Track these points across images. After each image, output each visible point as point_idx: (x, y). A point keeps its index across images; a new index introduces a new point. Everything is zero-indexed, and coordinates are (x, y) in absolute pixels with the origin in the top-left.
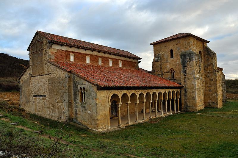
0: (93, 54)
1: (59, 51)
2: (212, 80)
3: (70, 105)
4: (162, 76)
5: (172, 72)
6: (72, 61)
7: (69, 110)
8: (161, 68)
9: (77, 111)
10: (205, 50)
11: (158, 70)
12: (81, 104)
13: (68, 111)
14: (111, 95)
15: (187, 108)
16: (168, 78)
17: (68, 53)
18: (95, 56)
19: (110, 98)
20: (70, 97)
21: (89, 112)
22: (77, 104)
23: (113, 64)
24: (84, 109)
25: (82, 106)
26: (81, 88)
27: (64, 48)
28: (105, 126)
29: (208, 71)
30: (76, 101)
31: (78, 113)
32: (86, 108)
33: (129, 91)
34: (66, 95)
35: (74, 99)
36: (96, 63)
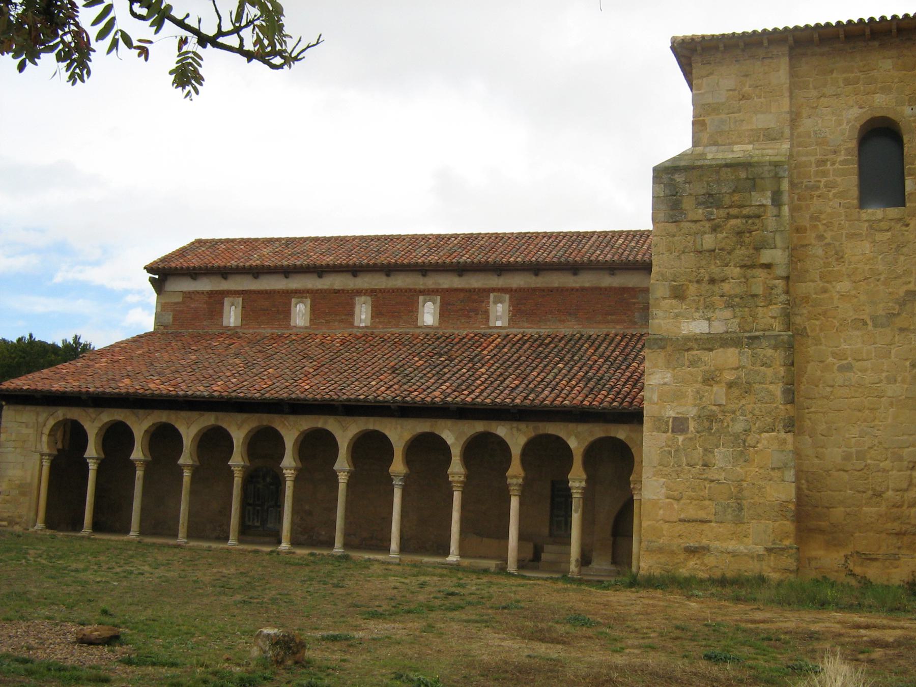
0: (326, 287)
1: (188, 295)
14: (51, 422)
17: (216, 299)
18: (337, 292)
19: (46, 431)
27: (205, 285)
36: (341, 321)
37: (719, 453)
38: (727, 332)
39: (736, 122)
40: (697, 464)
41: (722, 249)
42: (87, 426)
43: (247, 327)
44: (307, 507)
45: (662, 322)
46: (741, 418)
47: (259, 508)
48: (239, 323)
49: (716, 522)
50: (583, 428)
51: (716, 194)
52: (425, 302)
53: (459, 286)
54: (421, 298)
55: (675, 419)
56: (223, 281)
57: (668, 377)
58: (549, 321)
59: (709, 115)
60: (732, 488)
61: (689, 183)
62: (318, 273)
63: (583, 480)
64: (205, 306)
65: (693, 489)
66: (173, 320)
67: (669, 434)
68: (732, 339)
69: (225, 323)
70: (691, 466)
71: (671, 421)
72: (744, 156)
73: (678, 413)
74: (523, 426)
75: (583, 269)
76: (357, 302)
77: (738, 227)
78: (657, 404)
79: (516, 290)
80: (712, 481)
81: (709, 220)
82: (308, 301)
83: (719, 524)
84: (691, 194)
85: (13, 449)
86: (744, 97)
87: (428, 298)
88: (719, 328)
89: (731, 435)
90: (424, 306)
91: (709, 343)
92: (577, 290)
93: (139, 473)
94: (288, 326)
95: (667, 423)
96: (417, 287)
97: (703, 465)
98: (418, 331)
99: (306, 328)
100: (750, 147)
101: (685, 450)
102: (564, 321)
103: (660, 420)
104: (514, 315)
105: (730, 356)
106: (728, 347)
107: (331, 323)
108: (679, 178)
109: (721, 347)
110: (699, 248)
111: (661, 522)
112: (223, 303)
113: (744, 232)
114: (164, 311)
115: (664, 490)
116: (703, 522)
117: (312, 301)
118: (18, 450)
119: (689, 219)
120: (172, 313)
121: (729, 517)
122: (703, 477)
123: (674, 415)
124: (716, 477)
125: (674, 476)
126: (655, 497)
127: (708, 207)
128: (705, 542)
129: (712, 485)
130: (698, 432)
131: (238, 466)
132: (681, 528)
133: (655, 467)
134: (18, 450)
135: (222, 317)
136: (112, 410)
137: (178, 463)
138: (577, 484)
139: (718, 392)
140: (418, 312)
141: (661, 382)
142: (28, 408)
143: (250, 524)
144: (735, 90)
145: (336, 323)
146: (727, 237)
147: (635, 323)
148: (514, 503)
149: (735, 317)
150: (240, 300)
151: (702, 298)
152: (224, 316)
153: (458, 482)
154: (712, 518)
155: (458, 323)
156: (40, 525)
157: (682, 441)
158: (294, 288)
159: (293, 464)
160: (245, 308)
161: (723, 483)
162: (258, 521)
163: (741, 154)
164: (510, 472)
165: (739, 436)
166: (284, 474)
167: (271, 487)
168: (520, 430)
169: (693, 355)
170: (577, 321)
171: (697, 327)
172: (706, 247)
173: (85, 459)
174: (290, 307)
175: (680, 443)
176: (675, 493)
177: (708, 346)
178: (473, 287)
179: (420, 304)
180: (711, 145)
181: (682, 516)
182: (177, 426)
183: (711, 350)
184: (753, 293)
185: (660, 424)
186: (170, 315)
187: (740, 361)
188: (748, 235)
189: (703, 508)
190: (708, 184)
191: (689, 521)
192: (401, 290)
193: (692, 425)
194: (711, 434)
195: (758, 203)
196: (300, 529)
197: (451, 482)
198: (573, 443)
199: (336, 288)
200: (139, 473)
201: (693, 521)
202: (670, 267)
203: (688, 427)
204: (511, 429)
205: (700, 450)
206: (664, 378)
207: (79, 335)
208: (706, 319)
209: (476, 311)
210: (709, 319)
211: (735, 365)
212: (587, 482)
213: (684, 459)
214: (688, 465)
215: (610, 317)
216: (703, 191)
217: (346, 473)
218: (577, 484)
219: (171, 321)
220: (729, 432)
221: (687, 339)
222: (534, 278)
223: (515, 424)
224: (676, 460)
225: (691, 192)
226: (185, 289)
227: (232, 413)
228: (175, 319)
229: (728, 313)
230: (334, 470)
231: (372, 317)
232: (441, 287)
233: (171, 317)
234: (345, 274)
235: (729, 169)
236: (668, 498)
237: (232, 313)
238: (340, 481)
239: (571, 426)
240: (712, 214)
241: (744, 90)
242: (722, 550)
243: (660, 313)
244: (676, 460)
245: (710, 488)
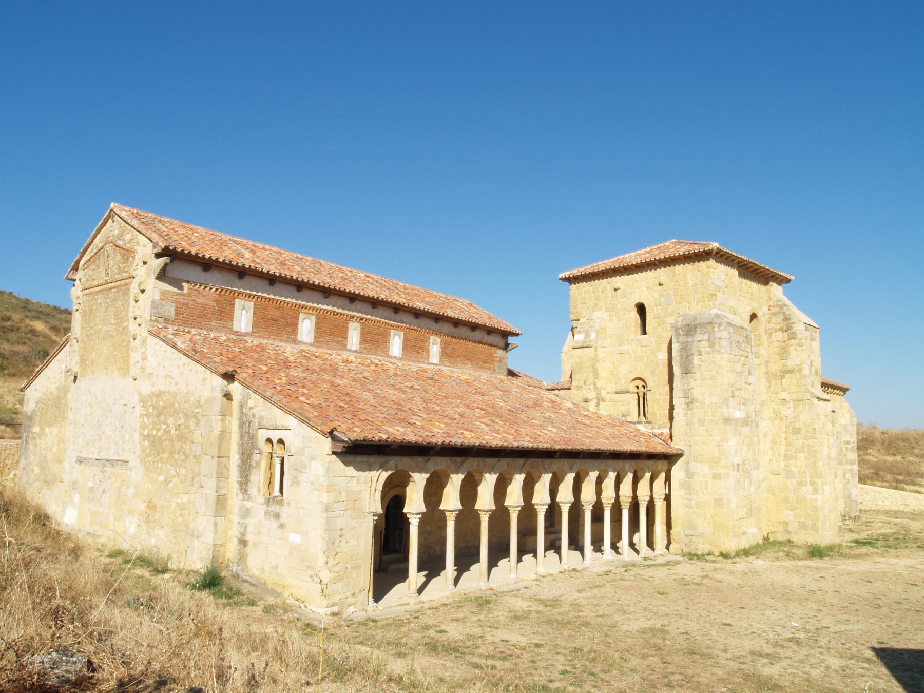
2: (797, 431)
3: (221, 503)
4: (598, 405)
5: (641, 395)
7: (215, 525)
8: (596, 374)
9: (249, 529)
10: (774, 310)
11: (585, 383)
12: (268, 502)
13: (212, 528)
15: (694, 539)
16: (623, 416)
20: (222, 474)
21: (295, 538)
22: (248, 504)
23: (403, 349)
24: (274, 524)
25: (267, 513)
26: (269, 441)
29: (784, 395)
30: (246, 491)
31: (250, 537)
32: (283, 519)
33: (459, 459)
34: (209, 465)
35: (241, 484)
36: (337, 342)
43: (257, 335)
48: (250, 330)
64: (214, 304)
66: (176, 313)
69: (235, 328)
76: (350, 327)
82: (314, 318)
87: (397, 332)
94: (295, 341)
98: (428, 367)
104: (442, 356)
112: (234, 304)
114: (164, 300)
117: (318, 318)
120: (174, 304)
135: (232, 319)
145: (334, 344)
150: (252, 304)
152: (234, 319)
154: (745, 516)
160: (256, 314)
173: (405, 515)
179: (392, 337)
186: (171, 306)
209: (421, 348)
215: (486, 365)
227: (518, 459)
228: (178, 312)
233: (173, 309)
237: (243, 317)
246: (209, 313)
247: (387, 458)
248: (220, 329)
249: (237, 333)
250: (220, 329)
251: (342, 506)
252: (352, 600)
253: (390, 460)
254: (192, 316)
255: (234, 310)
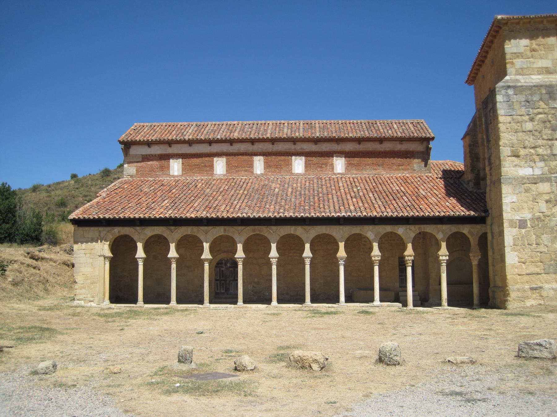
6: (176, 174)
28: (93, 297)
36: (246, 171)
37: (545, 237)
38: (542, 174)
39: (530, 63)
40: (533, 244)
41: (536, 131)
42: (236, 237)
44: (256, 280)
45: (508, 169)
46: (554, 219)
47: (224, 282)
48: (181, 173)
49: (545, 274)
50: (445, 227)
51: (530, 101)
52: (296, 159)
53: (316, 150)
54: (293, 157)
55: (520, 220)
56: (189, 148)
57: (514, 198)
58: (368, 169)
59: (515, 59)
60: (552, 255)
61: (516, 95)
62: (190, 144)
63: (447, 255)
65: (532, 257)
67: (517, 228)
68: (546, 178)
70: (530, 245)
71: (517, 221)
72: (541, 82)
73: (521, 217)
74: (412, 227)
75: (385, 141)
77: (544, 119)
78: (510, 213)
79: (348, 153)
80: (541, 253)
81: (528, 115)
83: (546, 275)
84: (517, 101)
85: (84, 255)
86: (534, 50)
88: (538, 172)
89: (549, 228)
90: (295, 161)
91: (535, 181)
92: (382, 153)
93: (174, 266)
94: (212, 174)
95: (516, 223)
96: (290, 151)
97: (536, 244)
99: (224, 175)
100: (540, 77)
101: (526, 237)
102: (376, 169)
103: (512, 221)
104: (348, 166)
105: (544, 187)
106: (544, 182)
107: (239, 172)
108: (510, 92)
109: (541, 182)
110: (524, 130)
111: (517, 275)
113: (546, 122)
115: (517, 259)
116: (538, 274)
118: (88, 255)
119: (518, 114)
121: (552, 271)
122: (538, 250)
123: (519, 218)
124: (544, 250)
125: (522, 250)
126: (512, 262)
127: (527, 108)
128: (540, 285)
129: (541, 254)
130: (532, 227)
131: (241, 258)
132: (526, 278)
133: (511, 246)
134: (88, 255)
136: (153, 228)
137: (136, 257)
138: (444, 258)
139: (543, 206)
140: (292, 165)
141: (511, 201)
142: (92, 228)
143: (219, 291)
144: (527, 46)
145: (243, 172)
146: (538, 124)
147: (414, 170)
148: (342, 269)
149: (546, 166)
151: (528, 156)
153: (377, 260)
154: (542, 271)
155: (316, 171)
156: (107, 301)
157: (525, 232)
158: (215, 152)
159: (277, 255)
160: (184, 164)
161: (547, 253)
162: (223, 290)
163: (538, 81)
164: (440, 253)
165: (553, 228)
166: (271, 261)
167: (231, 269)
168: (411, 230)
169: (526, 186)
170: (383, 169)
171: (526, 172)
172: (528, 129)
173: (136, 259)
174: (213, 163)
175: (523, 233)
176: (523, 260)
177: (533, 182)
178: (323, 150)
180: (517, 75)
181: (528, 272)
182: (198, 236)
183: (535, 183)
184: (554, 154)
185: (512, 224)
186: (134, 169)
187: (551, 189)
188: (548, 123)
189: (537, 267)
190: (526, 96)
191: (531, 274)
192: (152, 155)
193: (529, 223)
194: (539, 228)
195: (553, 107)
196: (252, 293)
197: (407, 261)
198: (440, 236)
199: (241, 152)
200: (174, 266)
201: (533, 274)
202: (510, 139)
203: (527, 225)
204: (406, 229)
205: (534, 236)
206: (512, 199)
207: (5, 182)
208: (531, 167)
210: (532, 167)
211: (549, 191)
212: (449, 256)
213: (526, 241)
214: (529, 244)
216: (524, 100)
217: (242, 259)
218: (444, 258)
219: (135, 172)
220: (548, 226)
221: (523, 178)
222: (358, 146)
223: (408, 226)
224: (522, 242)
225: (517, 100)
226: (144, 153)
229: (542, 164)
230: (469, 255)
231: (265, 168)
232: (305, 151)
233: (135, 170)
234: (290, 143)
235: (536, 88)
236: (519, 262)
238: (139, 264)
239: (439, 226)
240: (529, 111)
241: (533, 47)
242: (550, 288)
243: (507, 165)
244: (522, 242)
245: (541, 256)
246: (154, 169)
247: (113, 228)
248: (162, 176)
249: (173, 176)
250: (162, 176)
251: (83, 252)
252: (92, 299)
253: (114, 229)
254: (146, 172)
255: (170, 164)
